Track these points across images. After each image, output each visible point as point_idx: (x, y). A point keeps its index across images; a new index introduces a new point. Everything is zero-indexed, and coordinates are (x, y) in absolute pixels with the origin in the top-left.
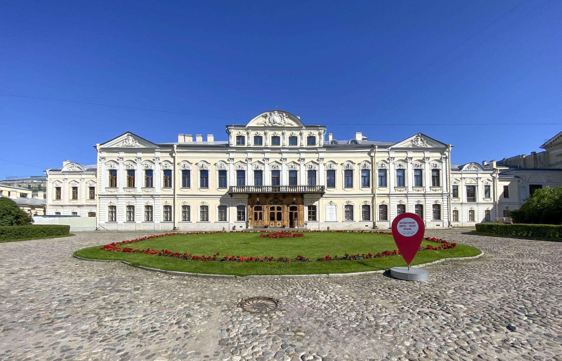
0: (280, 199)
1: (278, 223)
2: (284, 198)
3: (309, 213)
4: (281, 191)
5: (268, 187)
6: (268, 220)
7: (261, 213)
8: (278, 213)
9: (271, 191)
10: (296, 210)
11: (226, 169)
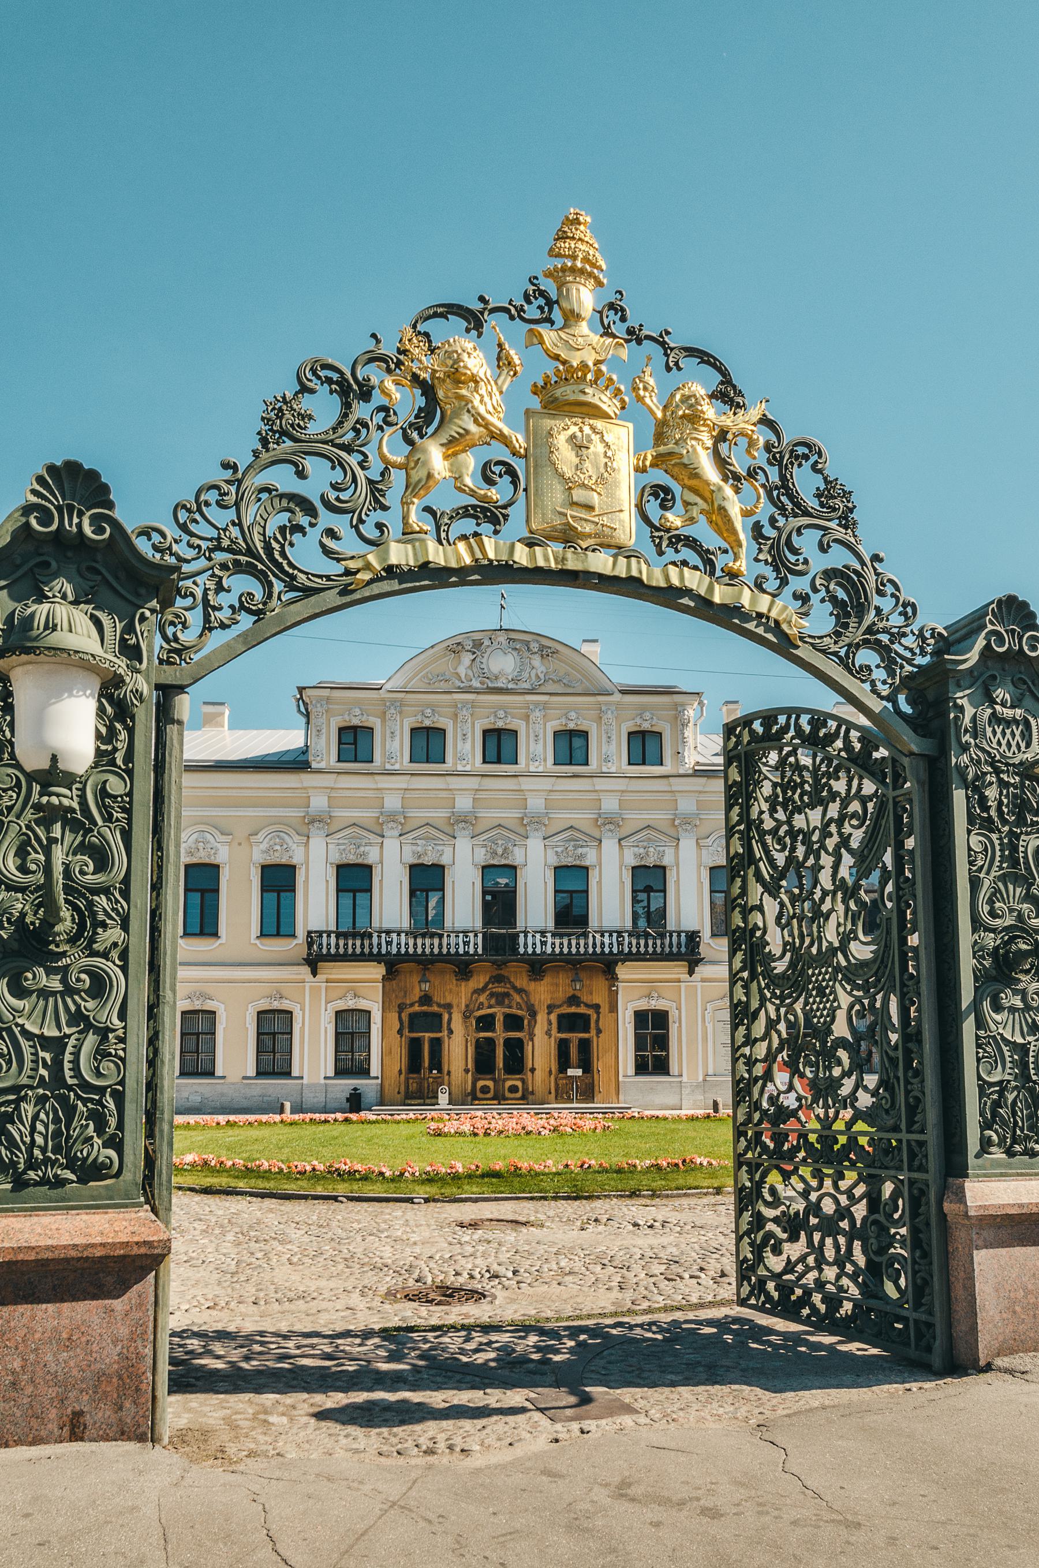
0: (518, 984)
1: (509, 1083)
2: (535, 980)
3: (640, 1044)
4: (522, 950)
5: (465, 933)
6: (467, 1071)
7: (437, 1045)
8: (508, 1042)
9: (480, 951)
10: (587, 1029)
11: (294, 861)
